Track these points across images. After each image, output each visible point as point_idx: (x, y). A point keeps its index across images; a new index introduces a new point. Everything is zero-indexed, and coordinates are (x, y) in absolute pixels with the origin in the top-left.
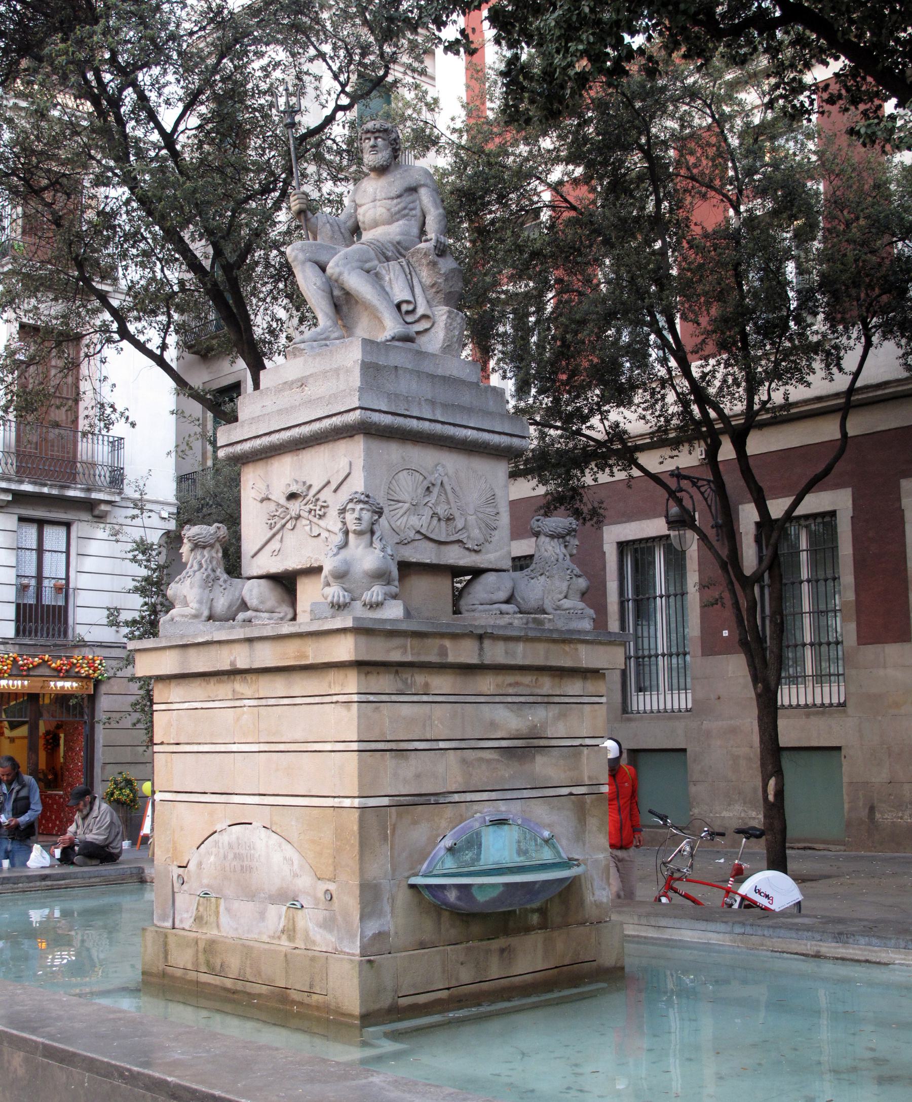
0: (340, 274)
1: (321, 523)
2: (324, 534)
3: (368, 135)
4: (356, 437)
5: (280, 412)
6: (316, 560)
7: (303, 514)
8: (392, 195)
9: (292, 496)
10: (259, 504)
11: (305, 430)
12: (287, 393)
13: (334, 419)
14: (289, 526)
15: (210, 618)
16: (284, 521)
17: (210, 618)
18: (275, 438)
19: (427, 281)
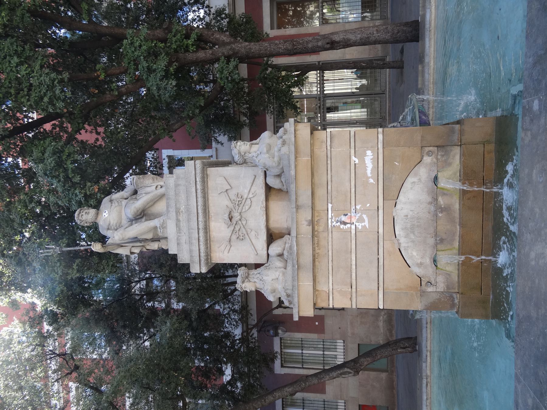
0: (135, 207)
1: (245, 197)
2: (251, 196)
3: (80, 215)
4: (208, 173)
5: (189, 220)
6: (262, 203)
7: (239, 211)
8: (110, 205)
9: (231, 219)
10: (232, 248)
11: (200, 200)
12: (181, 225)
13: (198, 180)
14: (244, 222)
15: (285, 269)
16: (242, 226)
17: (285, 269)
18: (201, 226)
19: (151, 181)
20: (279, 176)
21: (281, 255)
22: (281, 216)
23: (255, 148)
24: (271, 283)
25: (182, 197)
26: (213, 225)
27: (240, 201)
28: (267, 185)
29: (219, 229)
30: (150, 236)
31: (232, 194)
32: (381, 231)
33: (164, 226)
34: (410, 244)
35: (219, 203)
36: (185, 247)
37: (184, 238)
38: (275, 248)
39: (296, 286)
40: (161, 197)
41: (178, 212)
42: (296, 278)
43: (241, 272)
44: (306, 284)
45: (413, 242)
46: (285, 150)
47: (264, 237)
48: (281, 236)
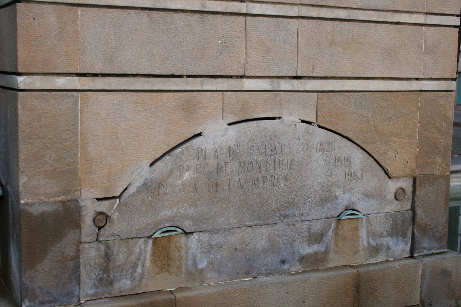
32: (249, 84)
34: (212, 162)
45: (219, 169)
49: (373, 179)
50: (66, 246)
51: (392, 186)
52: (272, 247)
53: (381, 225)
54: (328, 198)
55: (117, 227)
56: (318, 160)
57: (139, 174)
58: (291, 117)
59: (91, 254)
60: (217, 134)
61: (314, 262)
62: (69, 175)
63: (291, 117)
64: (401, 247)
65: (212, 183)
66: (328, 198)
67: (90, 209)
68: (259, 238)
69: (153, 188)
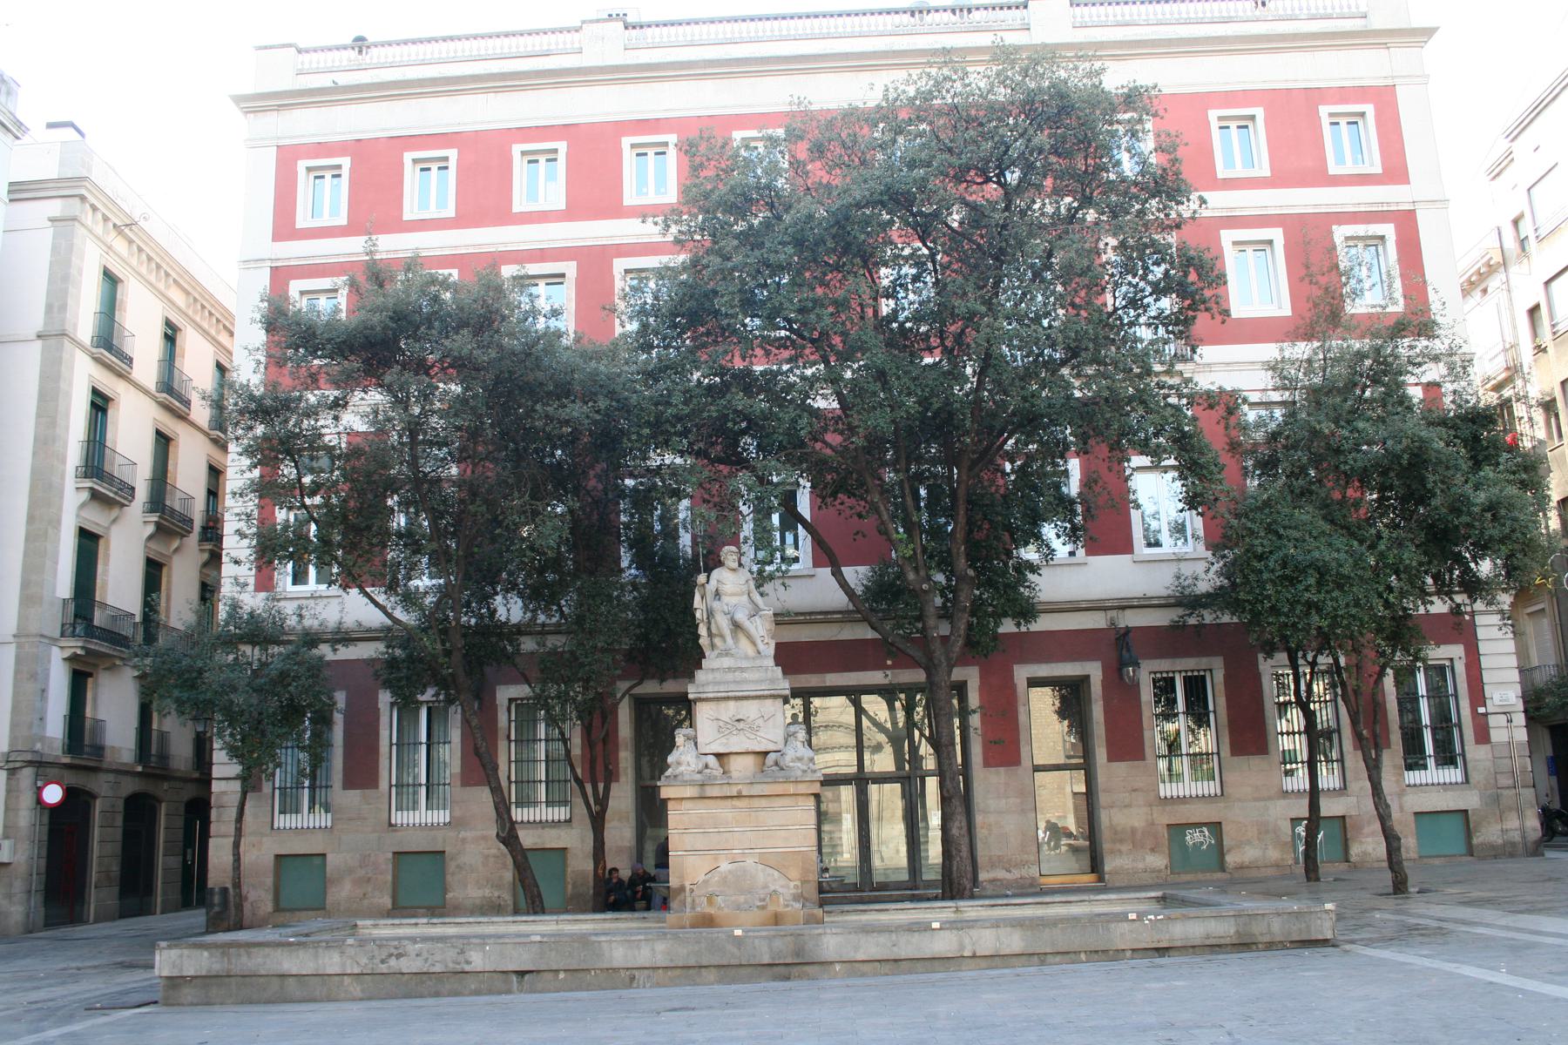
20: (776, 764)
21: (707, 766)
22: (742, 767)
23: (799, 745)
24: (684, 758)
25: (756, 675)
26: (732, 704)
27: (754, 729)
28: (766, 753)
29: (730, 710)
30: (714, 630)
31: (760, 722)
33: (726, 653)
35: (750, 710)
36: (710, 677)
37: (718, 676)
38: (712, 761)
39: (685, 783)
40: (754, 643)
41: (742, 669)
42: (692, 783)
43: (690, 731)
44: (689, 792)
46: (799, 773)
47: (722, 750)
48: (722, 766)
49: (783, 881)
50: (681, 897)
51: (792, 884)
52: (746, 902)
53: (789, 897)
54: (766, 887)
55: (696, 892)
56: (761, 875)
57: (701, 878)
58: (750, 861)
59: (689, 900)
60: (725, 866)
61: (763, 908)
62: (682, 877)
63: (750, 861)
64: (798, 906)
65: (724, 880)
66: (766, 887)
67: (688, 888)
68: (742, 899)
69: (706, 882)
